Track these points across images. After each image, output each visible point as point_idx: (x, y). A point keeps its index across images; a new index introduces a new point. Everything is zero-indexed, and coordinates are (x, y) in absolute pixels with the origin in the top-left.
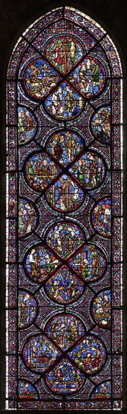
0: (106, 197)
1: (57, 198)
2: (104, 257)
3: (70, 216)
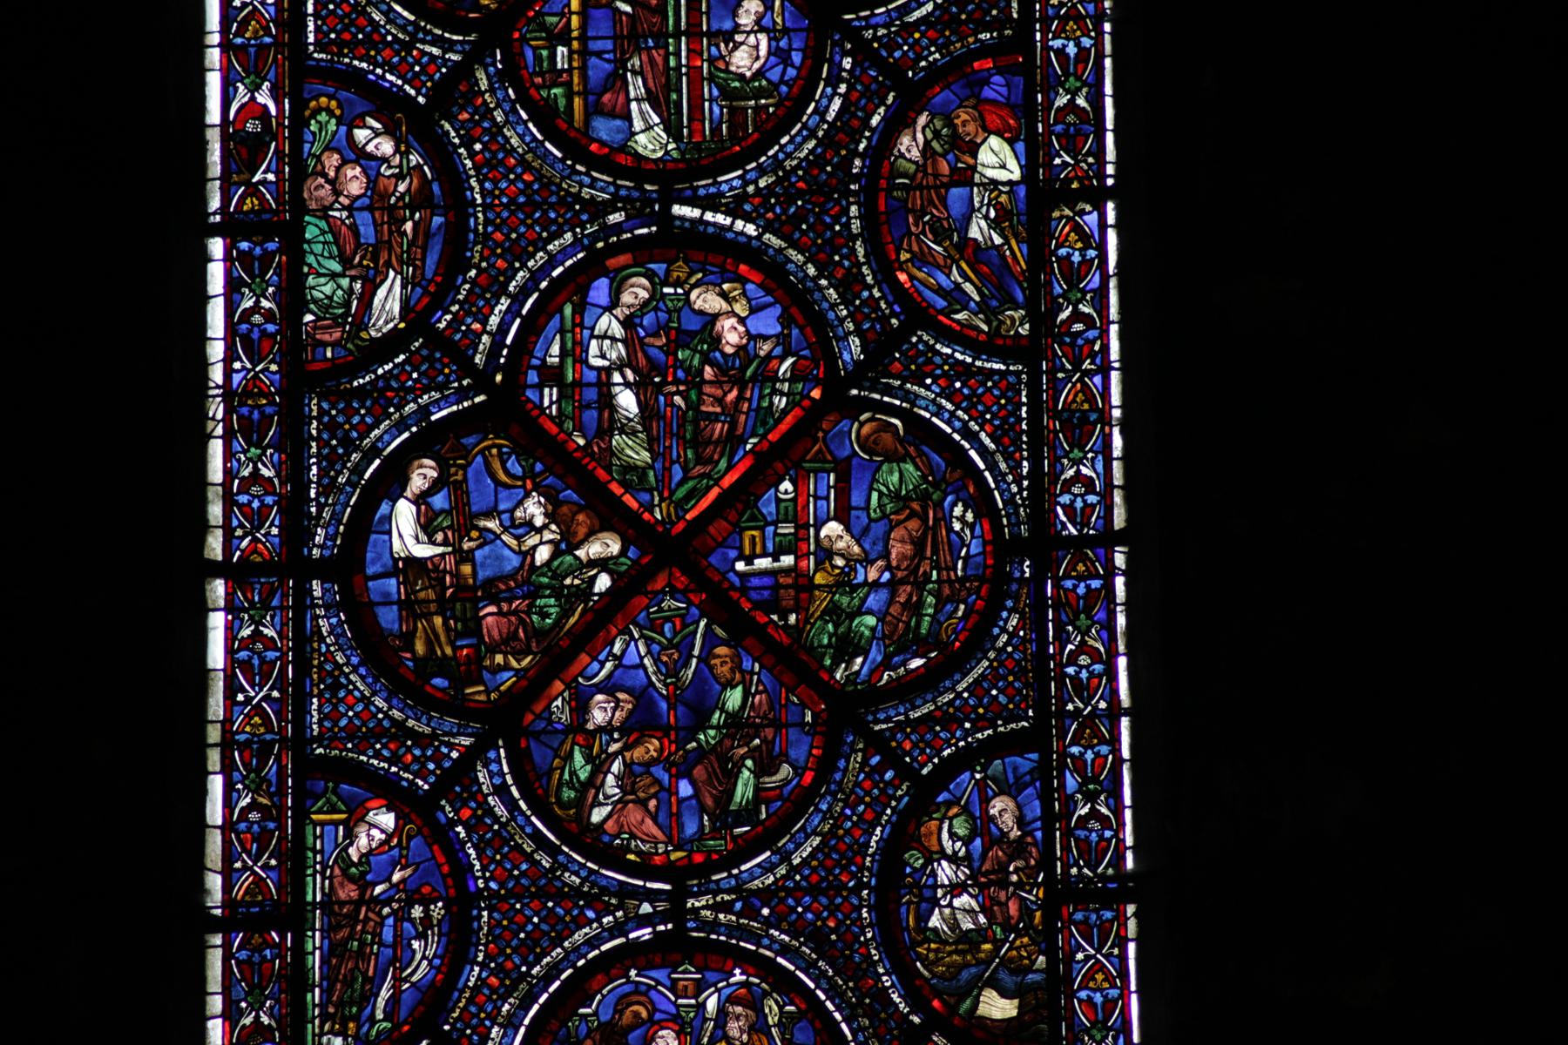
0: (984, 50)
1: (599, 68)
2: (981, 502)
3: (710, 203)
